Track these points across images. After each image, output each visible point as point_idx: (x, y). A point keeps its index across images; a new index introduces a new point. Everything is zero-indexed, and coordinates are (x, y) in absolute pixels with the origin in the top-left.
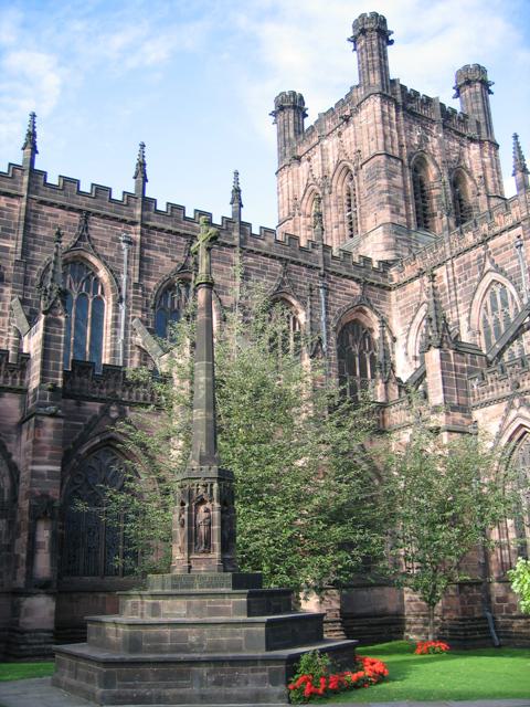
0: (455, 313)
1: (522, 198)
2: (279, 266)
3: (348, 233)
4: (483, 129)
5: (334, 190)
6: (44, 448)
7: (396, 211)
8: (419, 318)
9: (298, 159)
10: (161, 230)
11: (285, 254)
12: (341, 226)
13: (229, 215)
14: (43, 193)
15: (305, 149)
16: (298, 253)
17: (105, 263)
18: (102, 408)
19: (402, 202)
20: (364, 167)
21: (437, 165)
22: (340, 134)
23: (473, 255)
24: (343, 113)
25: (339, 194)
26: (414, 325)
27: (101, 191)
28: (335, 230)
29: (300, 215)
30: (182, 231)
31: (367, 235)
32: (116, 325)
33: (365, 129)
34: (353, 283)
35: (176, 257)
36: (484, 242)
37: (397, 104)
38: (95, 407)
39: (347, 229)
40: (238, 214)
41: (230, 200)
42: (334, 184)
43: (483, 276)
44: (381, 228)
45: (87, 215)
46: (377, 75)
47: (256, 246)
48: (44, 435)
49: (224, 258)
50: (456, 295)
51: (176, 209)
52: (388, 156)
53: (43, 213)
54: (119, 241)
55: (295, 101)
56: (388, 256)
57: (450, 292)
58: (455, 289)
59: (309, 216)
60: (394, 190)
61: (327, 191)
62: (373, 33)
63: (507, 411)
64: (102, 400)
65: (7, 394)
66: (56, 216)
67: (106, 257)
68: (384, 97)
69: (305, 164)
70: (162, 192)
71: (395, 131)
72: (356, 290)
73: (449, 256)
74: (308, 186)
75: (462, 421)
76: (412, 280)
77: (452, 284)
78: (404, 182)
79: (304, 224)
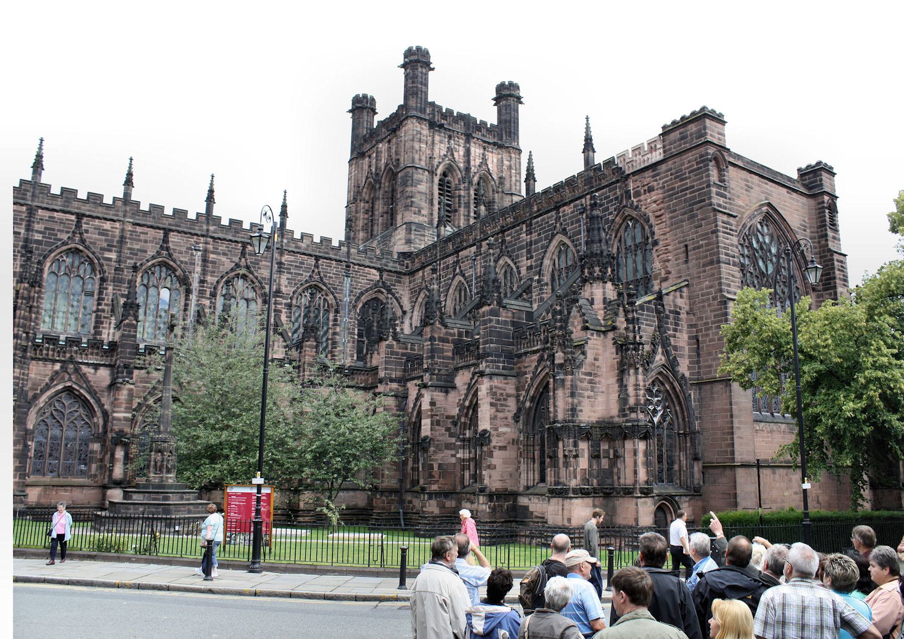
2: (312, 261)
3: (389, 222)
5: (382, 186)
6: (121, 403)
8: (420, 300)
10: (224, 239)
11: (319, 252)
14: (138, 217)
15: (368, 146)
16: (331, 252)
22: (389, 142)
23: (451, 260)
25: (386, 189)
26: (417, 304)
27: (180, 214)
28: (380, 219)
29: (361, 201)
30: (239, 240)
31: (396, 229)
33: (403, 143)
36: (457, 252)
42: (383, 181)
43: (454, 276)
44: (405, 226)
47: (296, 247)
48: (122, 395)
53: (137, 232)
54: (192, 250)
59: (367, 202)
60: (418, 195)
61: (377, 186)
65: (102, 368)
66: (147, 234)
67: (182, 262)
72: (375, 275)
74: (367, 178)
75: (397, 389)
76: (418, 270)
79: (364, 208)
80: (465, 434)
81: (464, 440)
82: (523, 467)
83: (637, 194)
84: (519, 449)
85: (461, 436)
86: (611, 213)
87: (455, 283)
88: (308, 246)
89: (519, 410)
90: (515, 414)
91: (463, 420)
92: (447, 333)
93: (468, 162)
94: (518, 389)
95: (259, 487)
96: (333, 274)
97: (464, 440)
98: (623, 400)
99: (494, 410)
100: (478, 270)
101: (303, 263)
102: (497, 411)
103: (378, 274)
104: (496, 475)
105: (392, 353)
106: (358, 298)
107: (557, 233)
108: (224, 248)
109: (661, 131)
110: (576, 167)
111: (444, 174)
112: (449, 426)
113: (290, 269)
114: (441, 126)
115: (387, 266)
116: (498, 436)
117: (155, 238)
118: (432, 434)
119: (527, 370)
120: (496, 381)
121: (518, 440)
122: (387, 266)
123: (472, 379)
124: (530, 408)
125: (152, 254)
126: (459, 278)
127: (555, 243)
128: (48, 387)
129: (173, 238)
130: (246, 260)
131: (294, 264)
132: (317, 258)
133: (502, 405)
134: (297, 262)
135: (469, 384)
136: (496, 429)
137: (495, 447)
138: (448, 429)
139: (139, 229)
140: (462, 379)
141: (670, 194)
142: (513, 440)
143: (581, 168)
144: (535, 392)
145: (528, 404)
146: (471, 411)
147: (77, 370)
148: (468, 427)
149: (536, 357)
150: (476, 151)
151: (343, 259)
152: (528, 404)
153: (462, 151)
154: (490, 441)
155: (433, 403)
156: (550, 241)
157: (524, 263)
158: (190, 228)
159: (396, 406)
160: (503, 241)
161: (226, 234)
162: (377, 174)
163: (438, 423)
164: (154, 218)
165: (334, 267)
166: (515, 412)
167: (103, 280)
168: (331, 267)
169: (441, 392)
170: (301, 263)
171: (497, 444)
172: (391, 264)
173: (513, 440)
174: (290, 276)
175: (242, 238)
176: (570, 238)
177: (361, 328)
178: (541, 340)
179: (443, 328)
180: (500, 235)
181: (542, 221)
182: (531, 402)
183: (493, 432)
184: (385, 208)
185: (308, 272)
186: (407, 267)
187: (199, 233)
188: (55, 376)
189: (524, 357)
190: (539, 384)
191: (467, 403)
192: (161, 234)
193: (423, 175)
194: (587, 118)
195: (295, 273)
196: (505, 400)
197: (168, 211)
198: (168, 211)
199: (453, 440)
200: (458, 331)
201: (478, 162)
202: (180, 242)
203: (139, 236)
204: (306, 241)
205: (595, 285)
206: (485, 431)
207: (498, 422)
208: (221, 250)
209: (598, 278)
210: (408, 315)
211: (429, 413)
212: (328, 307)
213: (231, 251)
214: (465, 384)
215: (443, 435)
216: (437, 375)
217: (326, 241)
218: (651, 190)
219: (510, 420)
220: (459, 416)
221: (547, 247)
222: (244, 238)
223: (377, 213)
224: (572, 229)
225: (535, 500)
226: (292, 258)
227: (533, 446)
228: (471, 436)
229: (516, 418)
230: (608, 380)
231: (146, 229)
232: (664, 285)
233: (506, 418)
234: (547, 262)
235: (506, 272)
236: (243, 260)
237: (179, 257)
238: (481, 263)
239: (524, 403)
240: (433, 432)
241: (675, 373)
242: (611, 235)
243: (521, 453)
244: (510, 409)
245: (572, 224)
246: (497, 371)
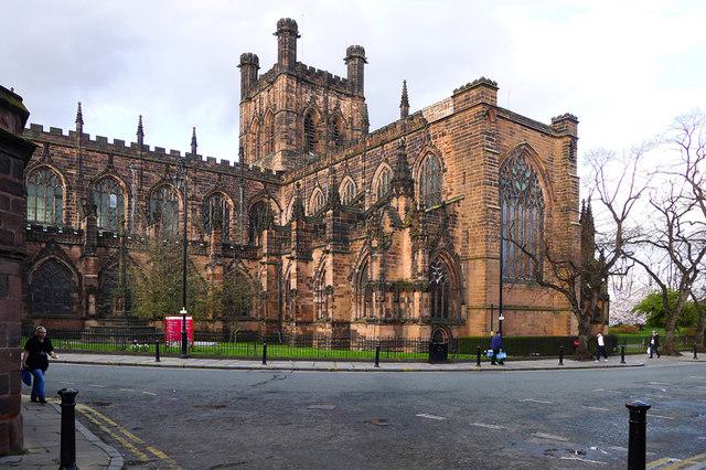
7: (290, 143)
23: (312, 177)
27: (119, 143)
40: (194, 150)
45: (111, 156)
62: (288, 32)
70: (152, 142)
72: (261, 186)
82: (353, 307)
83: (435, 137)
87: (315, 192)
93: (327, 106)
95: (184, 315)
98: (414, 267)
104: (337, 312)
106: (249, 202)
110: (395, 115)
111: (309, 116)
114: (307, 81)
126: (317, 189)
127: (380, 168)
128: (38, 259)
129: (117, 160)
132: (220, 174)
140: (316, 255)
141: (456, 138)
143: (397, 117)
145: (357, 271)
147: (58, 248)
149: (362, 242)
150: (332, 99)
153: (321, 99)
155: (297, 269)
157: (360, 181)
160: (347, 166)
163: (301, 281)
167: (69, 188)
188: (43, 251)
192: (107, 157)
194: (405, 82)
201: (333, 106)
206: (330, 286)
207: (338, 281)
210: (285, 212)
217: (225, 163)
218: (444, 134)
225: (360, 326)
229: (350, 278)
230: (406, 257)
232: (449, 198)
234: (374, 181)
241: (452, 254)
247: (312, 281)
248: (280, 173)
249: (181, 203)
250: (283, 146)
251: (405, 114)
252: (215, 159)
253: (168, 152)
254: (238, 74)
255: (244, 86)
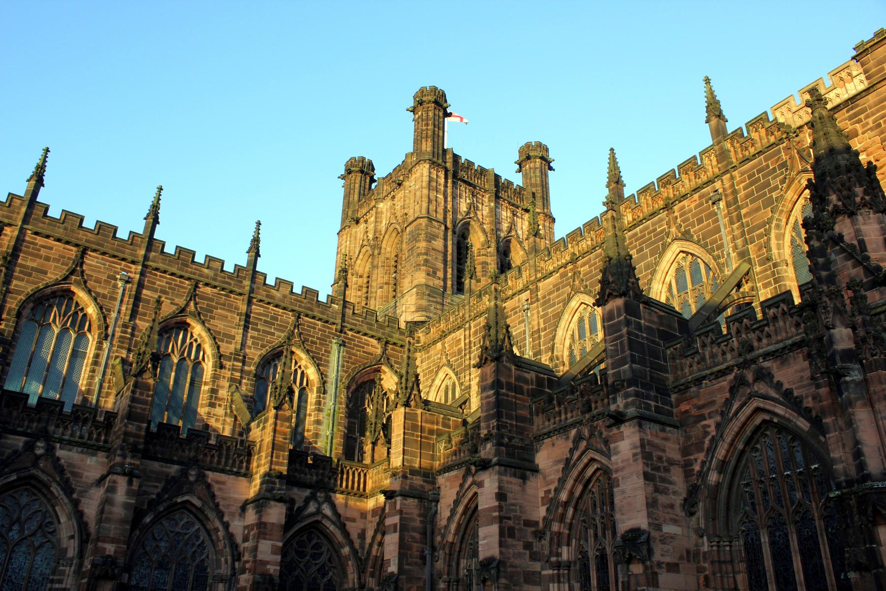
0: (467, 378)
1: (532, 262)
2: (291, 318)
3: (392, 294)
4: (539, 203)
5: (383, 251)
7: (432, 274)
9: (357, 222)
11: (300, 306)
12: (385, 287)
13: (244, 263)
14: (41, 225)
15: (364, 211)
17: (95, 299)
18: (26, 443)
19: (440, 265)
20: (408, 229)
21: (484, 231)
22: (393, 197)
24: (398, 177)
25: (388, 255)
26: (433, 388)
27: (105, 230)
30: (187, 275)
31: (403, 296)
32: (96, 363)
34: (374, 342)
35: (177, 300)
37: (447, 171)
38: (19, 442)
39: (391, 290)
41: (247, 249)
42: (384, 246)
46: (430, 143)
47: (267, 296)
49: (230, 306)
50: (470, 359)
51: (185, 255)
52: (430, 220)
53: (36, 244)
54: (116, 279)
55: (363, 166)
56: (418, 317)
57: (465, 355)
58: (470, 353)
59: (361, 277)
60: (432, 253)
61: (376, 252)
63: (465, 478)
64: (23, 434)
66: (51, 249)
67: (98, 294)
68: (433, 164)
69: (362, 226)
71: (441, 196)
73: (467, 319)
74: (362, 246)
75: (422, 486)
76: (435, 342)
77: (468, 347)
78: (446, 246)
80: (559, 555)
81: (558, 566)
84: (700, 570)
85: (553, 559)
86: (776, 188)
88: (284, 296)
89: (693, 492)
90: (685, 500)
91: (555, 527)
92: (519, 378)
94: (685, 451)
96: (317, 338)
97: (558, 566)
99: (650, 489)
100: (535, 323)
101: (277, 319)
102: (657, 490)
103: (379, 346)
105: (414, 427)
107: (673, 240)
108: (164, 284)
109: (854, 53)
112: (530, 540)
113: (257, 324)
115: (392, 337)
116: (663, 541)
117: (64, 257)
118: (501, 553)
119: (706, 411)
120: (648, 431)
121: (697, 554)
122: (392, 337)
123: (571, 451)
124: (718, 485)
125: (54, 277)
127: (669, 255)
129: (92, 260)
130: (196, 304)
131: (263, 318)
133: (663, 480)
134: (267, 316)
135: (568, 461)
136: (658, 527)
137: (659, 564)
138: (528, 546)
139: (40, 240)
142: (688, 552)
144: (728, 451)
145: (713, 477)
146: (571, 511)
148: (565, 540)
149: (725, 382)
151: (332, 320)
152: (713, 477)
154: (650, 552)
155: (501, 496)
156: (662, 254)
158: (117, 250)
159: (420, 515)
160: (576, 274)
161: (168, 265)
162: (376, 238)
164: (66, 229)
165: (320, 330)
166: (684, 495)
168: (315, 328)
169: (515, 476)
170: (272, 318)
171: (662, 559)
172: (397, 336)
173: (688, 552)
174: (256, 334)
175: (191, 273)
176: (698, 243)
177: (353, 420)
178: (732, 350)
179: (513, 367)
180: (570, 267)
181: (641, 231)
182: (720, 473)
183: (655, 534)
184: (386, 277)
185: (283, 331)
186: (418, 342)
187: (130, 258)
189: (694, 389)
190: (738, 434)
191: (564, 496)
192: (73, 252)
193: (438, 229)
195: (264, 331)
196: (667, 470)
197: (89, 224)
198: (89, 224)
199: (537, 566)
200: (537, 377)
202: (100, 267)
203: (39, 250)
204: (285, 290)
205: (860, 218)
206: (635, 532)
208: (158, 285)
209: (865, 205)
211: (496, 514)
212: (307, 385)
213: (174, 289)
214: (557, 462)
215: (519, 555)
216: (507, 446)
217: (310, 293)
219: (679, 511)
220: (547, 521)
221: (657, 264)
222: (194, 274)
223: (374, 284)
224: (700, 230)
226: (261, 310)
227: (732, 562)
228: (572, 558)
229: (689, 505)
231: (51, 242)
233: (672, 506)
235: (581, 320)
236: (192, 304)
237: (95, 287)
238: (538, 312)
239: (703, 475)
240: (503, 550)
242: (780, 220)
243: (706, 578)
244: (676, 488)
245: (700, 221)
246: (648, 413)
247: (539, 535)
248: (414, 326)
249: (208, 367)
250: (421, 277)
251: (719, 132)
252: (291, 285)
253: (200, 258)
254: (336, 192)
255: (347, 204)
